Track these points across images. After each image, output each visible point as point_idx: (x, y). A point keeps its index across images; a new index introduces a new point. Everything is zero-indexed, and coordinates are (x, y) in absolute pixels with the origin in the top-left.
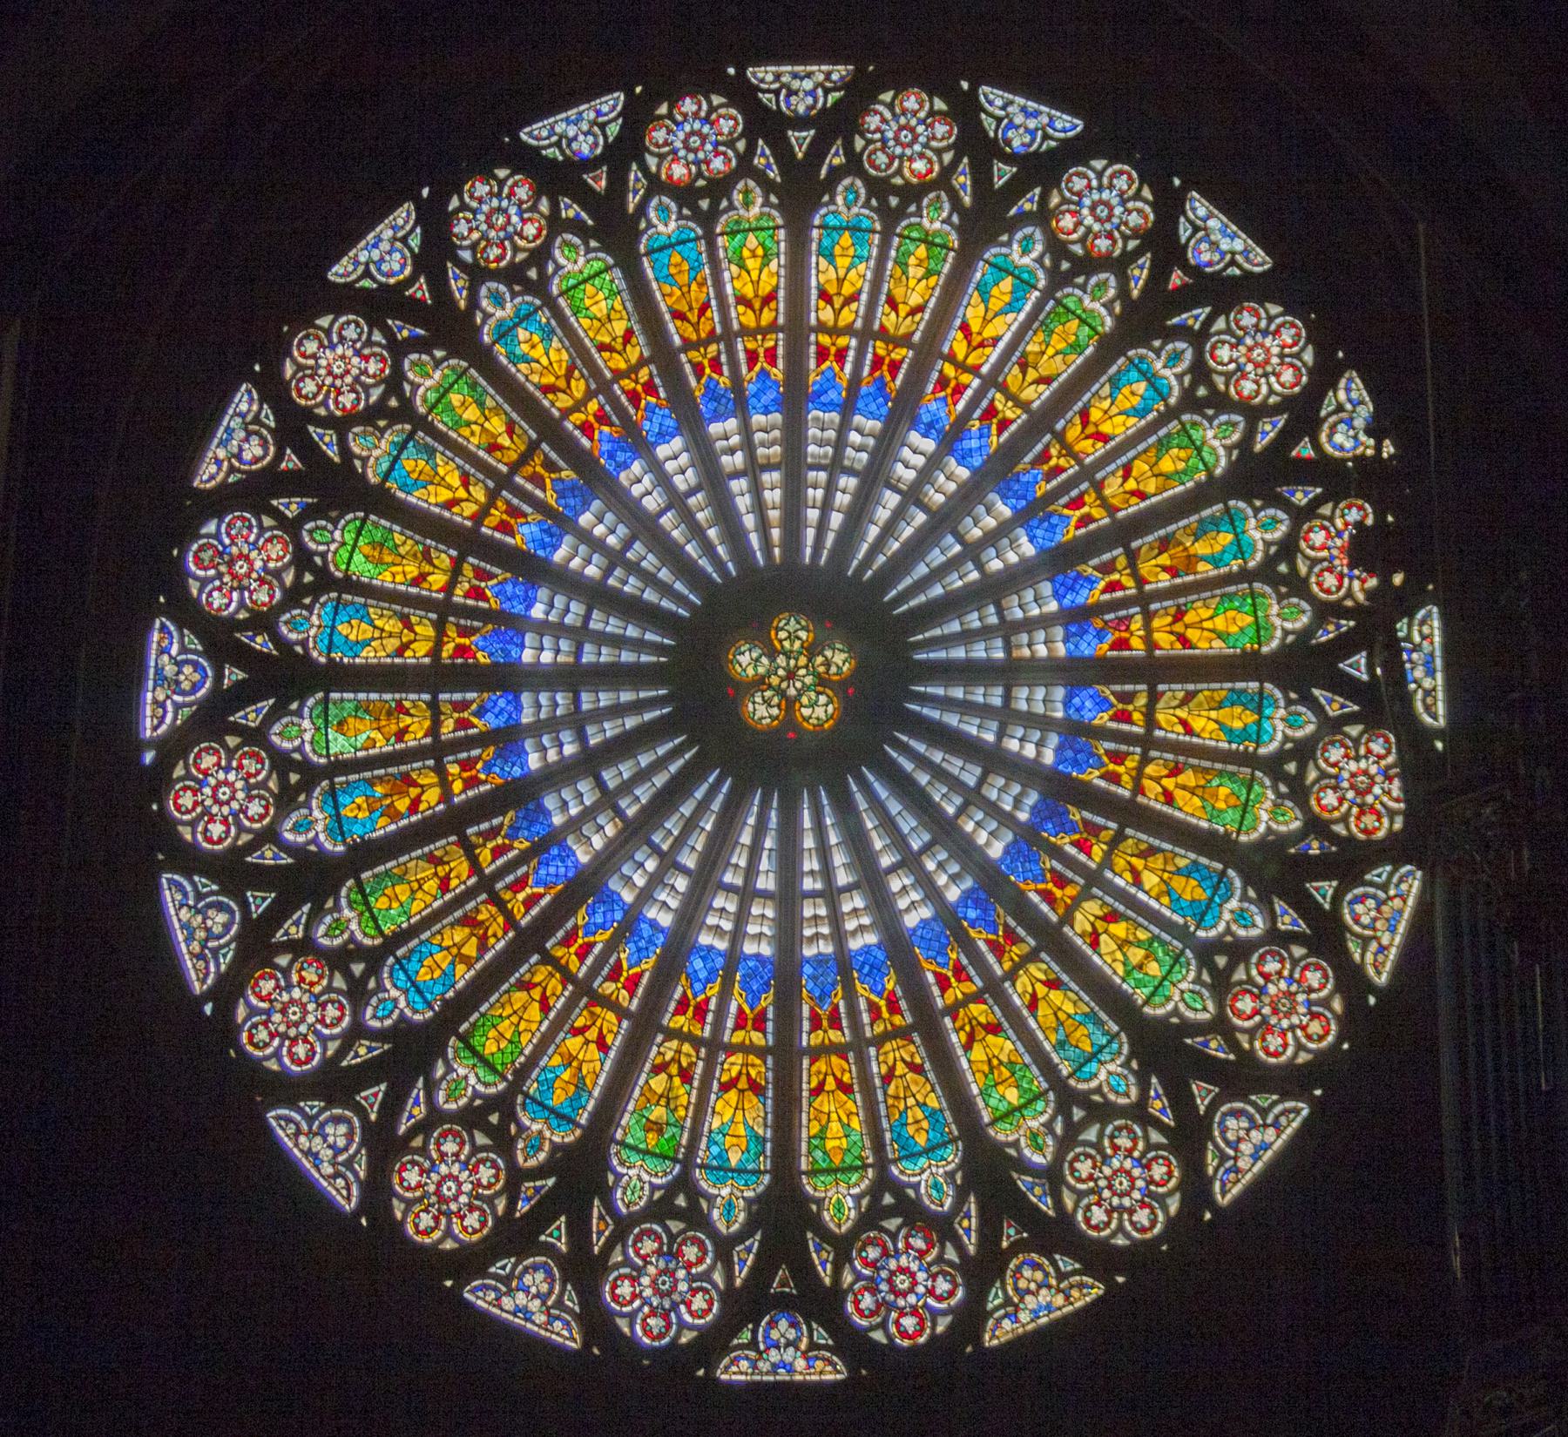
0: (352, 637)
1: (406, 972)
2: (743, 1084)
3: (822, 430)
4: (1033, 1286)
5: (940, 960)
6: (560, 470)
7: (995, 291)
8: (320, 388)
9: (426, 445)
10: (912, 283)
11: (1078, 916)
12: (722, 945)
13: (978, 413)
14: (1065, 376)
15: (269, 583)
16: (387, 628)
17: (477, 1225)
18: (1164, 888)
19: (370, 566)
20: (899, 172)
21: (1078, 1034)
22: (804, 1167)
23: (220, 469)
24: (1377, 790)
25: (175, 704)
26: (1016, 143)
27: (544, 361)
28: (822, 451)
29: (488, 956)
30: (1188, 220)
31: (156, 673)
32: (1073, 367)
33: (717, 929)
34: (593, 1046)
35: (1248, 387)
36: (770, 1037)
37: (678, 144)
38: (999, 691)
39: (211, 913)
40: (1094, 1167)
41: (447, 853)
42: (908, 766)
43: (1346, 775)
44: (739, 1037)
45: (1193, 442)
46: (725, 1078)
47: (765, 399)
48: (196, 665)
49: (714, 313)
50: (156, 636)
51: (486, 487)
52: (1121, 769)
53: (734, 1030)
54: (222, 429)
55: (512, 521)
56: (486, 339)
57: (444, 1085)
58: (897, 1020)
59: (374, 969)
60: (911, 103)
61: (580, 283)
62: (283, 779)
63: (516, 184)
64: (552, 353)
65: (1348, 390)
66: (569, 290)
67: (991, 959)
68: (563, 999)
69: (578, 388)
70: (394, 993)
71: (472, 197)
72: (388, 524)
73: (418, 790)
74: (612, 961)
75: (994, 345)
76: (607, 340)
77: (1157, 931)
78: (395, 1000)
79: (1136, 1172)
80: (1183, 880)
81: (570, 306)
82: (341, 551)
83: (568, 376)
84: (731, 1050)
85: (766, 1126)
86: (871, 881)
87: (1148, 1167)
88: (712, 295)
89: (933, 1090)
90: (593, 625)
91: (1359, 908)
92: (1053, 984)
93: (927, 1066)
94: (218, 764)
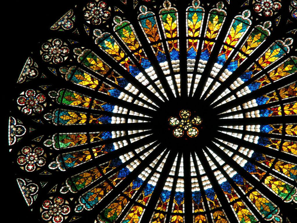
0: (64, 119)
3: (191, 63)
5: (229, 191)
7: (238, 27)
8: (50, 57)
9: (81, 71)
10: (214, 25)
11: (266, 180)
12: (170, 190)
13: (234, 58)
16: (73, 117)
18: (288, 172)
19: (68, 101)
21: (266, 208)
23: (24, 79)
25: (16, 137)
27: (112, 49)
28: (191, 69)
29: (107, 195)
30: (291, 6)
31: (10, 130)
32: (260, 45)
33: (168, 186)
34: (136, 215)
38: (242, 126)
39: (31, 187)
41: (94, 171)
42: (218, 145)
44: (175, 212)
47: (175, 56)
48: (21, 128)
50: (10, 121)
51: (98, 81)
52: (276, 144)
53: (174, 210)
54: (23, 69)
55: (106, 89)
58: (218, 206)
61: (121, 28)
62: (48, 155)
63: (101, 3)
64: (114, 46)
67: (242, 191)
68: (127, 204)
70: (82, 204)
71: (89, 7)
72: (72, 91)
74: (140, 195)
76: (130, 42)
77: (287, 183)
78: (82, 206)
80: (294, 170)
82: (59, 98)
83: (119, 52)
84: (174, 214)
86: (210, 173)
88: (159, 30)
90: (130, 114)
93: (226, 217)
94: (29, 151)
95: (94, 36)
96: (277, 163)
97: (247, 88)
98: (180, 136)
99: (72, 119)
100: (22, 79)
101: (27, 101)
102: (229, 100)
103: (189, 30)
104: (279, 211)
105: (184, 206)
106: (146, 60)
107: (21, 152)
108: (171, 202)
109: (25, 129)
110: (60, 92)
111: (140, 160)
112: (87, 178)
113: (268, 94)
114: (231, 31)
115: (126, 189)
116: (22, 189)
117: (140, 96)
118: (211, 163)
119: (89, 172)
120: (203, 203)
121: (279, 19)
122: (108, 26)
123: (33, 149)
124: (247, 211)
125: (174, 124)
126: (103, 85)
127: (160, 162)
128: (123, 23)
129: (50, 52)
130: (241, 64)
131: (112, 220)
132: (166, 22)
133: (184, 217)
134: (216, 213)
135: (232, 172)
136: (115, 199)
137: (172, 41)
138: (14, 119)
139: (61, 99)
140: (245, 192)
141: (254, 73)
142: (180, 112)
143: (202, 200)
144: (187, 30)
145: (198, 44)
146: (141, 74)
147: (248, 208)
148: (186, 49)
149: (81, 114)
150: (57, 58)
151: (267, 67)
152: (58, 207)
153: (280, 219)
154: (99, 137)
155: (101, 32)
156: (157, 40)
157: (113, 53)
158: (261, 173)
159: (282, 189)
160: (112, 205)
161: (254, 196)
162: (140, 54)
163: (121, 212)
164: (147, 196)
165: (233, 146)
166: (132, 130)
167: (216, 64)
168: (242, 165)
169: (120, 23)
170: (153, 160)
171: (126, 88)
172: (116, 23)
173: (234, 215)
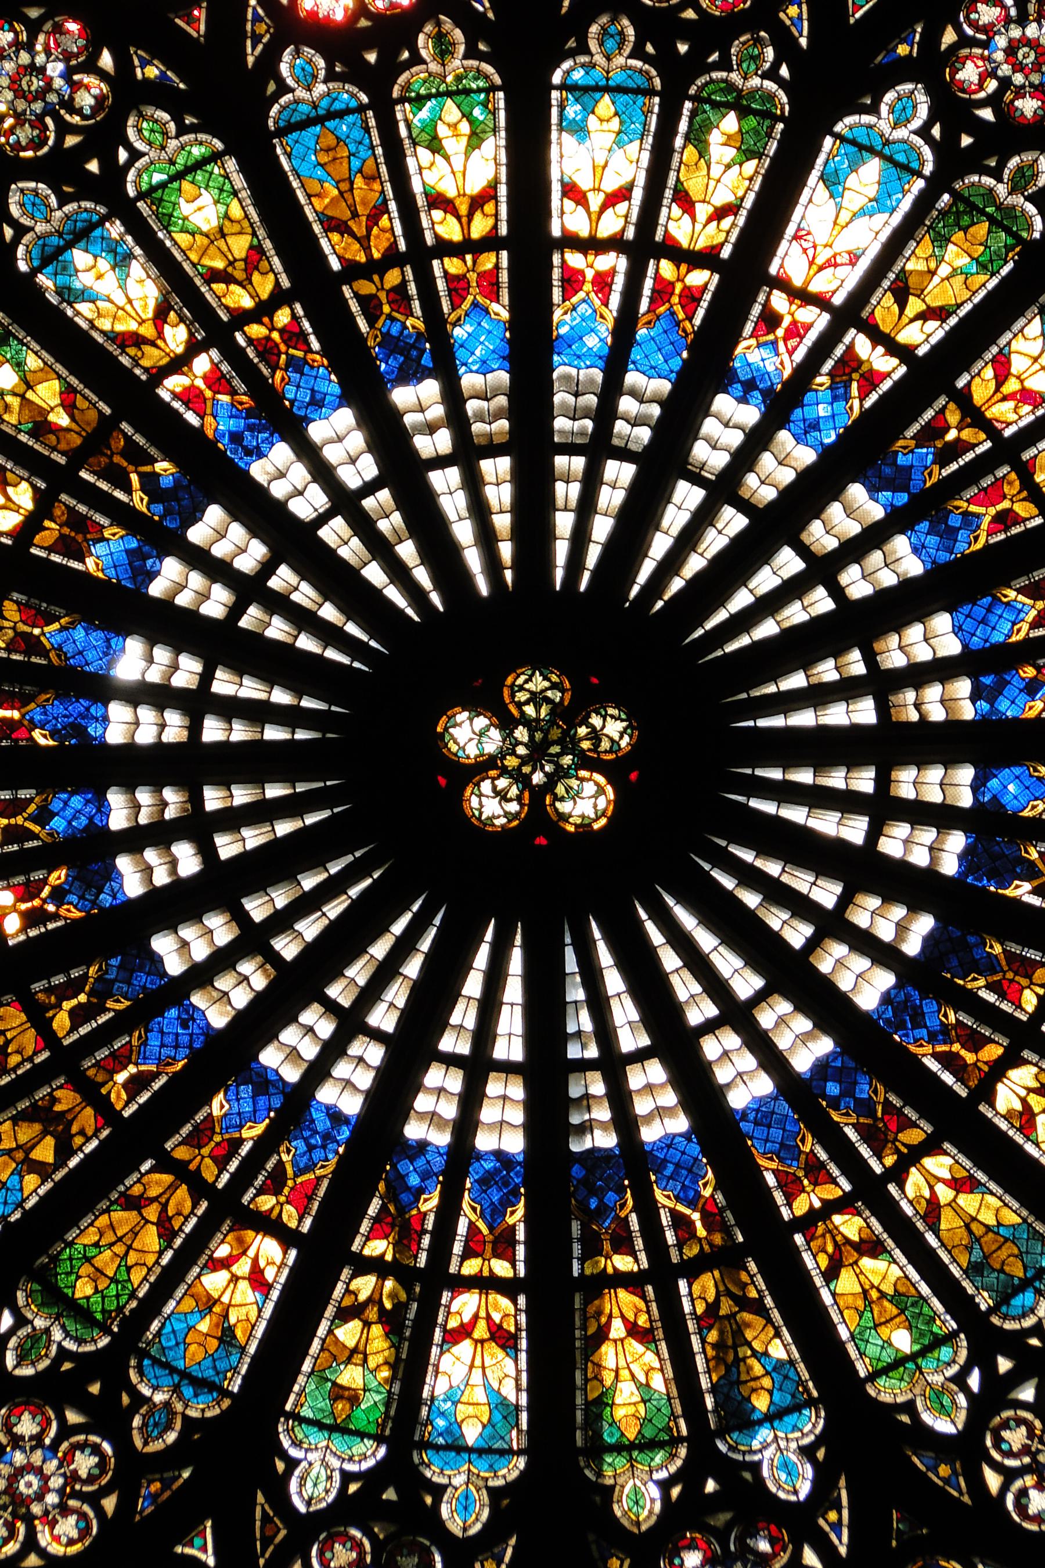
2: (481, 1331)
3: (576, 395)
6: (153, 461)
7: (852, 181)
10: (716, 170)
12: (442, 1139)
14: (968, 307)
17: (74, 1534)
21: (1003, 1254)
22: (579, 1442)
29: (73, 1163)
32: (982, 293)
33: (433, 1118)
34: (244, 1285)
40: (1031, 1435)
42: (728, 882)
44: (471, 1267)
46: (453, 1323)
49: (393, 221)
51: (34, 487)
53: (465, 1257)
55: (80, 538)
56: (23, 266)
57: (13, 1342)
66: (153, 189)
67: (865, 1151)
68: (194, 1220)
69: (176, 337)
74: (270, 1165)
75: (853, 262)
76: (219, 264)
84: (462, 1284)
85: (518, 1389)
88: (390, 194)
89: (778, 1334)
92: (961, 1185)
93: (769, 1301)
95: (14, 223)
97: (901, 544)
98: (503, 820)
102: (795, 614)
105: (521, 1235)
106: (312, 367)
108: (448, 1212)
113: (1022, 582)
117: (274, 583)
120: (633, 1218)
122: (93, 166)
125: (472, 751)
126: (57, 512)
130: (868, 403)
131: (103, 1311)
132: (435, 146)
133: (522, 1300)
134: (707, 1284)
135: (804, 1038)
136: (122, 1188)
137: (469, 258)
140: (880, 1159)
141: (945, 456)
142: (509, 680)
143: (630, 1203)
145: (619, 283)
146: (281, 453)
147: (898, 1253)
151: (1022, 423)
154: (32, 818)
155: (53, 201)
156: (376, 255)
157: (119, 328)
158: (975, 1049)
160: (103, 1220)
161: (932, 1180)
162: (282, 331)
163: (157, 1262)
165: (814, 884)
166: (225, 783)
167: (723, 403)
168: (868, 1000)
169: (163, 148)
170: (349, 962)
171: (197, 534)
172: (140, 146)
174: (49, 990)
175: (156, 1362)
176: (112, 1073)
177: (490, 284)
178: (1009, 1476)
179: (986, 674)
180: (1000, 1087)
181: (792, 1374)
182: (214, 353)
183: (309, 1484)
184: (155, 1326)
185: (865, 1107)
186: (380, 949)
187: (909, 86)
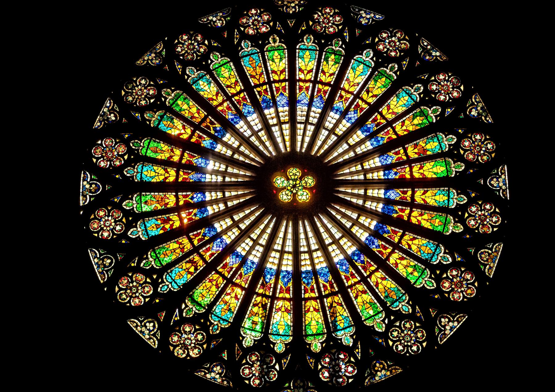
1: (171, 277)
2: (283, 309)
3: (302, 112)
4: (380, 369)
6: (215, 124)
8: (134, 99)
10: (330, 66)
13: (353, 106)
15: (120, 159)
17: (197, 353)
20: (325, 30)
21: (392, 294)
23: (101, 124)
24: (488, 220)
25: (90, 196)
26: (363, 23)
27: (209, 91)
31: (83, 187)
34: (233, 299)
35: (442, 98)
36: (291, 295)
37: (250, 24)
39: (105, 260)
40: (398, 333)
41: (183, 241)
43: (477, 215)
44: (281, 295)
45: (425, 115)
46: (277, 307)
47: (283, 103)
48: (96, 184)
50: (82, 176)
52: (403, 214)
55: (200, 140)
57: (185, 311)
59: (160, 276)
60: (328, 10)
62: (127, 219)
65: (475, 98)
66: (216, 68)
68: (223, 285)
70: (167, 283)
71: (182, 40)
73: (172, 222)
74: (239, 273)
75: (358, 86)
76: (229, 84)
77: (416, 263)
78: (168, 285)
79: (412, 335)
81: (216, 74)
82: (143, 149)
84: (279, 299)
87: (416, 333)
88: (264, 70)
91: (483, 256)
92: (383, 279)
93: (343, 304)
94: (105, 214)
96: (404, 238)
98: (287, 200)
99: (158, 176)
100: (99, 124)
101: (105, 151)
103: (299, 71)
104: (408, 298)
107: (95, 215)
109: (101, 187)
110: (144, 142)
111: (239, 228)
112: (174, 250)
113: (393, 151)
114: (350, 74)
115: (222, 265)
116: (94, 262)
118: (325, 235)
119: (177, 242)
121: (406, 62)
123: (109, 211)
124: (368, 297)
125: (281, 185)
127: (263, 231)
128: (222, 60)
129: (133, 92)
132: (273, 60)
133: (292, 302)
134: (330, 299)
138: (87, 173)
139: (145, 151)
142: (288, 171)
143: (314, 282)
144: (297, 71)
145: (311, 88)
146: (242, 123)
147: (370, 294)
148: (296, 94)
149: (169, 170)
150: (142, 101)
152: (138, 285)
153: (409, 309)
155: (195, 71)
159: (410, 270)
160: (204, 285)
162: (242, 98)
164: (247, 275)
168: (363, 239)
169: (218, 60)
171: (225, 139)
173: (352, 302)
174: (193, 235)
175: (215, 315)
176: (206, 253)
177: (284, 88)
178: (394, 342)
179: (386, 171)
180: (391, 258)
181: (348, 319)
182: (228, 102)
183: (247, 342)
184: (215, 308)
185: (363, 262)
186: (262, 227)
187: (369, 50)
